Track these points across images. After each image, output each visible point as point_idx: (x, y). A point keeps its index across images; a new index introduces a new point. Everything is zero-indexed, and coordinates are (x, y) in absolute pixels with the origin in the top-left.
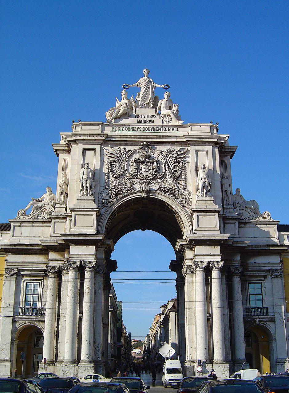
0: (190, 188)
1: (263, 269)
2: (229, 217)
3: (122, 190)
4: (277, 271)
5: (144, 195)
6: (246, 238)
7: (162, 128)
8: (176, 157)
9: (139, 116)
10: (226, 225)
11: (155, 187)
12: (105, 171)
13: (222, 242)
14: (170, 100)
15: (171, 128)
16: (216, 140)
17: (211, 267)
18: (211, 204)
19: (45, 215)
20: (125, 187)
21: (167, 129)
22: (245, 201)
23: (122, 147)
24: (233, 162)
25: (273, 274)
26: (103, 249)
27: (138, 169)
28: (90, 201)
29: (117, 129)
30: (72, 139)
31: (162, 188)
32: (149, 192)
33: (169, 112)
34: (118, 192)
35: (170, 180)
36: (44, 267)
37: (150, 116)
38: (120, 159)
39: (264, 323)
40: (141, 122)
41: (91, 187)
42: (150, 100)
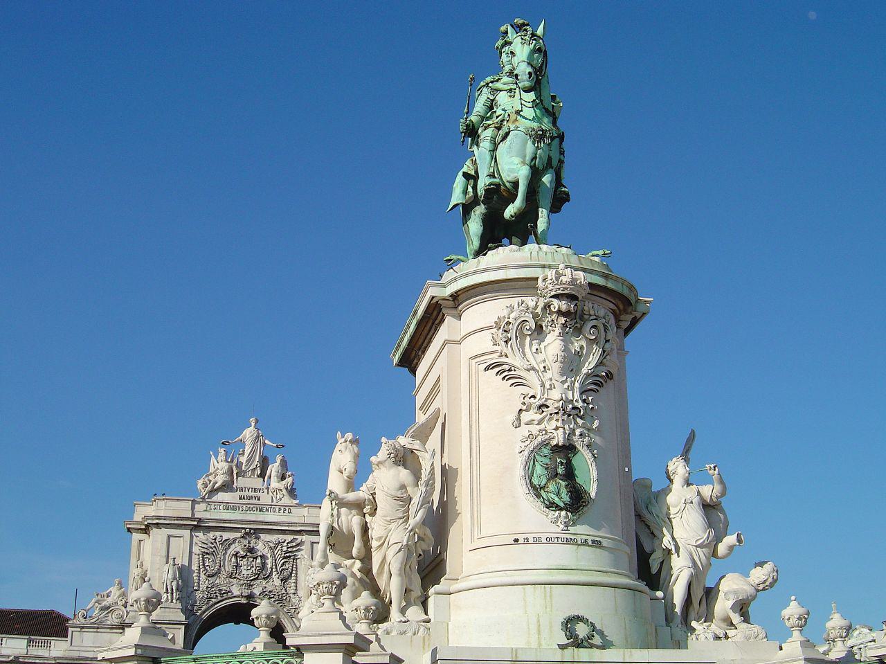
0: (300, 593)
3: (215, 593)
9: (241, 490)
11: (257, 591)
12: (195, 567)
14: (284, 464)
19: (113, 619)
23: (218, 534)
27: (237, 566)
28: (176, 610)
29: (213, 507)
30: (155, 522)
33: (281, 485)
35: (277, 582)
37: (256, 490)
38: (214, 551)
41: (177, 589)
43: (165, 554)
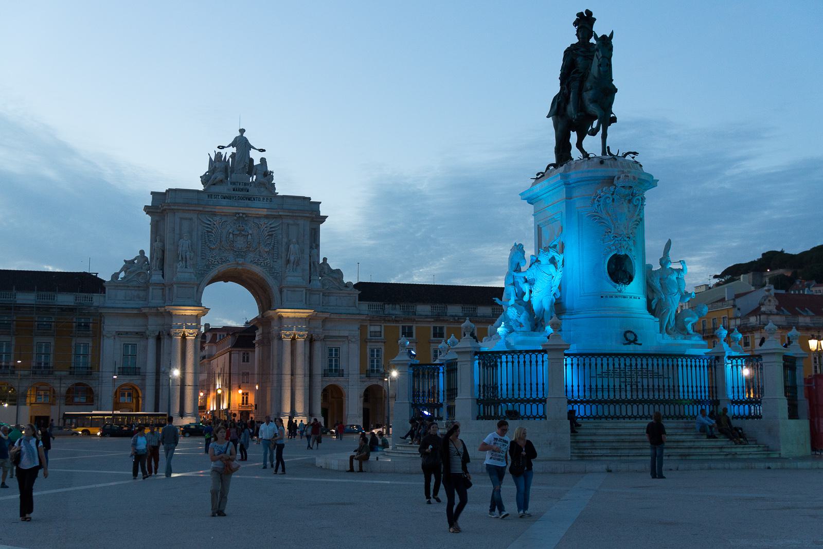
5: (240, 268)
16: (308, 215)
21: (262, 199)
37: (245, 184)
40: (236, 190)
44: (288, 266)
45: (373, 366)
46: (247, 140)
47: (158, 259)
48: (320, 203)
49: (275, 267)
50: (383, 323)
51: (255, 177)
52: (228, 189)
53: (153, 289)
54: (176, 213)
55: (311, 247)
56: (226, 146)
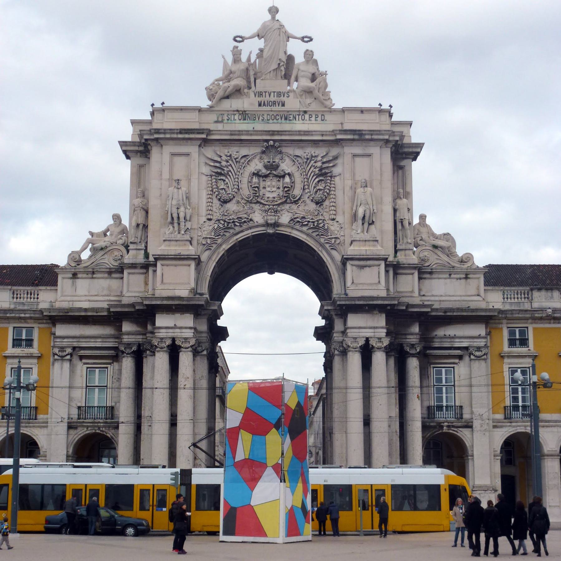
1: (457, 345)
2: (404, 264)
4: (479, 349)
5: (270, 231)
6: (433, 296)
7: (299, 115)
8: (321, 166)
10: (398, 276)
13: (389, 308)
15: (314, 116)
16: (386, 137)
17: (371, 346)
18: (374, 246)
20: (238, 218)
22: (433, 235)
24: (417, 168)
25: (472, 354)
26: (206, 317)
29: (225, 118)
31: (298, 219)
32: (276, 225)
34: (228, 225)
36: (115, 343)
37: (279, 94)
39: (455, 429)
40: (264, 105)
42: (279, 64)
43: (166, 175)
44: (354, 227)
45: (515, 399)
46: (282, 26)
47: (138, 225)
48: (410, 124)
49: (332, 228)
50: (532, 323)
51: (295, 85)
52: (252, 104)
53: (129, 273)
54: (164, 146)
55: (396, 197)
56: (246, 35)
